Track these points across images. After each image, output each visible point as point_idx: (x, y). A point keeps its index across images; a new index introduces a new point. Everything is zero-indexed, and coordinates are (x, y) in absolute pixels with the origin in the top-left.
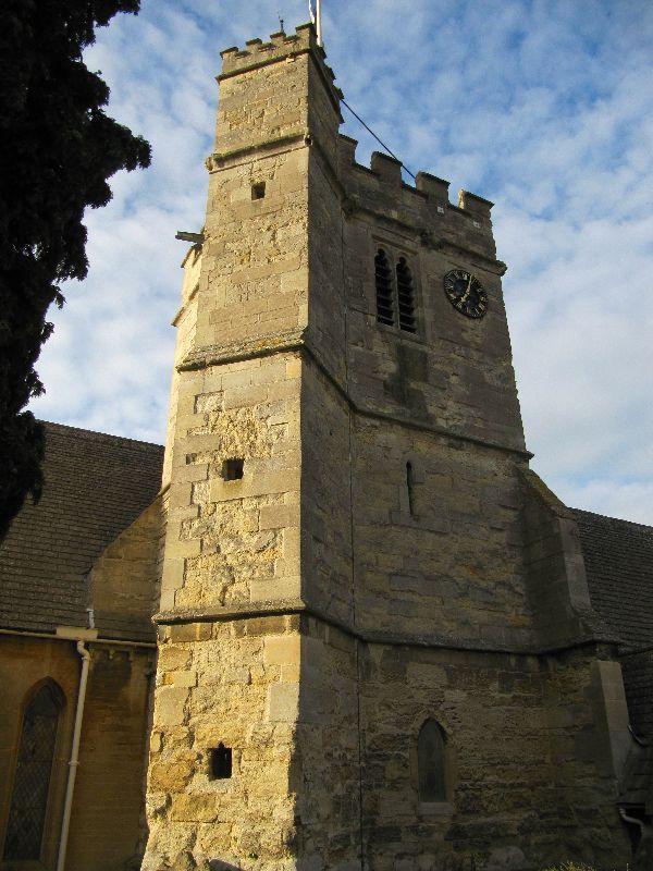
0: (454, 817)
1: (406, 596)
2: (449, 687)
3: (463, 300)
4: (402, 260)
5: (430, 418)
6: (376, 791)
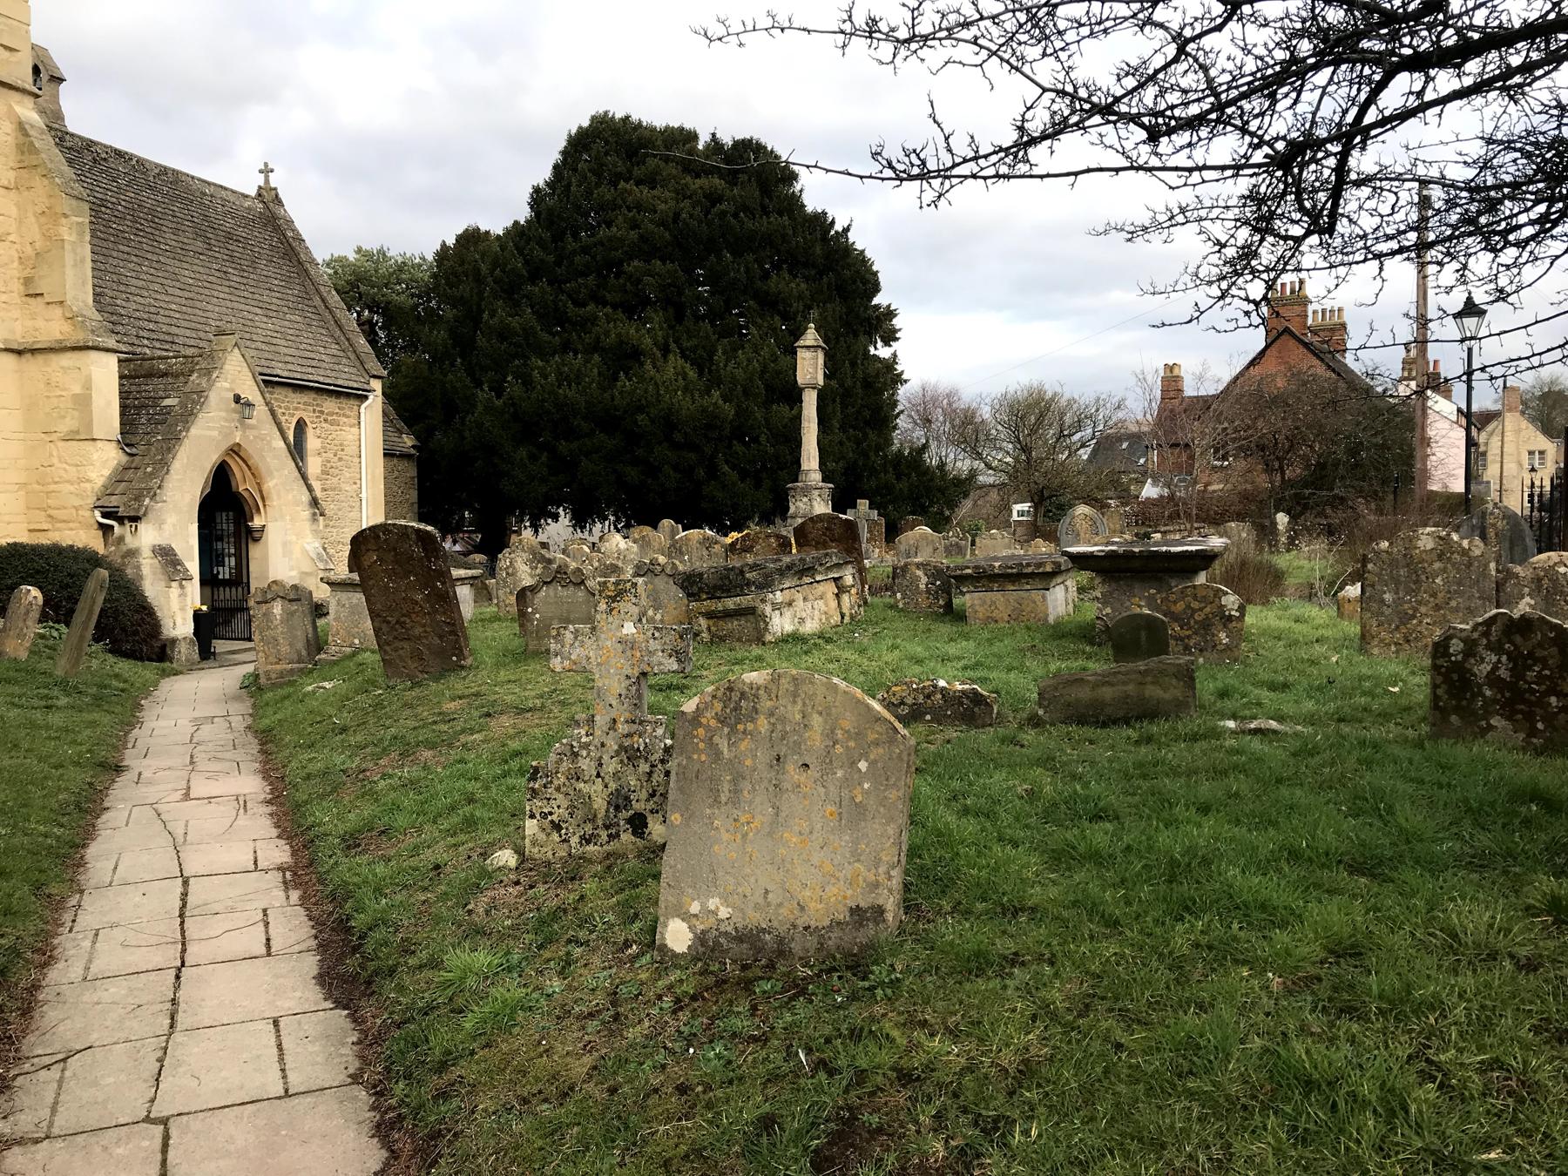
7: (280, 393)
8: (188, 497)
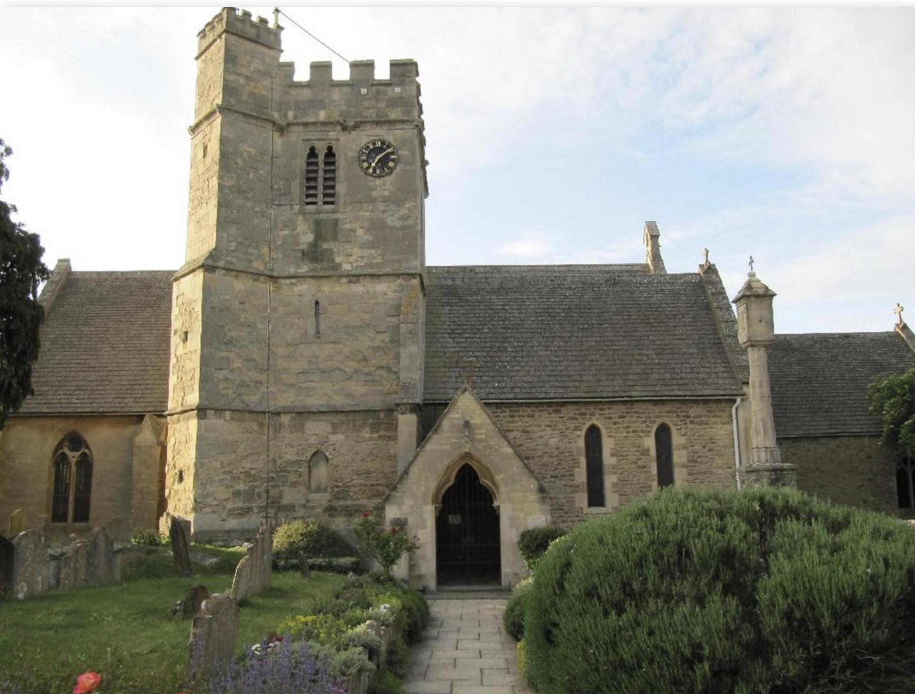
0: (330, 501)
2: (332, 433)
3: (373, 165)
4: (330, 149)
5: (336, 267)
6: (282, 488)
7: (504, 415)
8: (422, 489)
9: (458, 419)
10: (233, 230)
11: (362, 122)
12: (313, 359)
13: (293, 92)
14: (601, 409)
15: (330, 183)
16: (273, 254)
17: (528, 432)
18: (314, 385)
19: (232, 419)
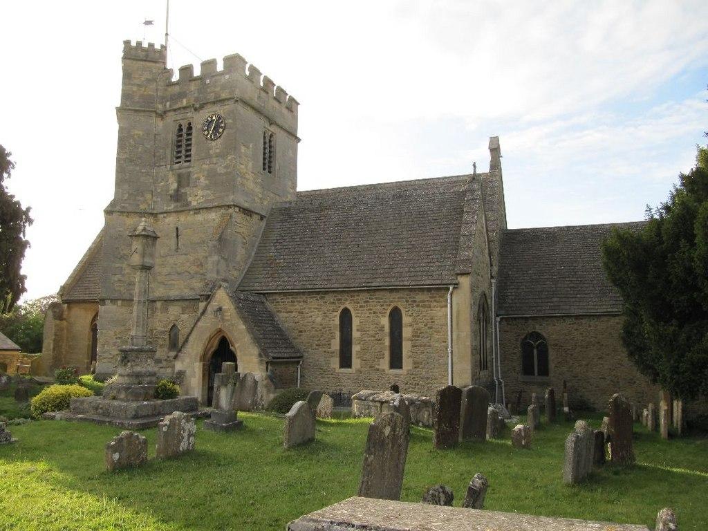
1: (170, 282)
4: (190, 124)
5: (188, 204)
8: (195, 352)
9: (215, 305)
10: (126, 186)
11: (204, 104)
12: (174, 266)
13: (170, 89)
14: (352, 296)
15: (189, 148)
16: (155, 199)
17: (302, 313)
18: (173, 282)
19: (122, 305)
